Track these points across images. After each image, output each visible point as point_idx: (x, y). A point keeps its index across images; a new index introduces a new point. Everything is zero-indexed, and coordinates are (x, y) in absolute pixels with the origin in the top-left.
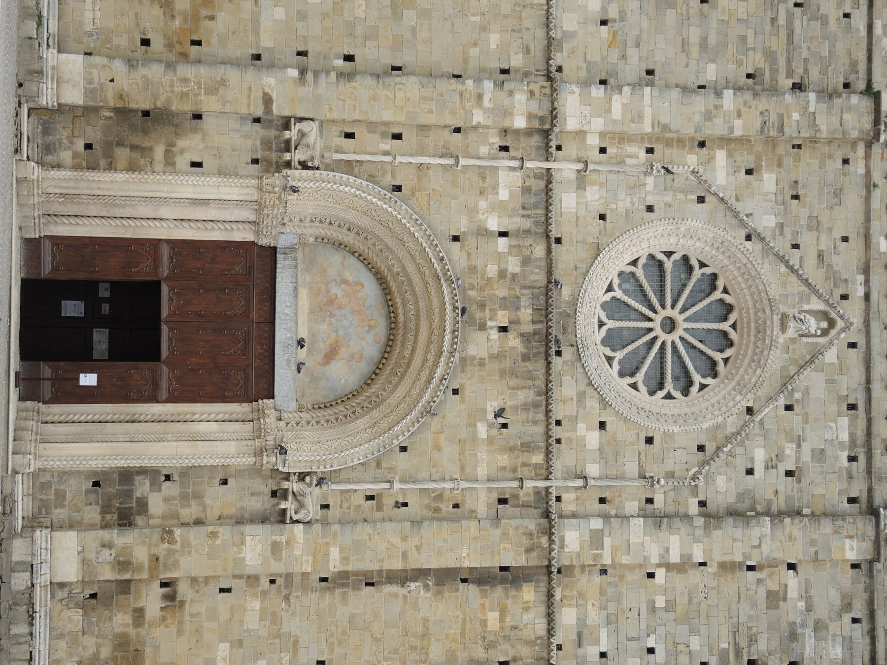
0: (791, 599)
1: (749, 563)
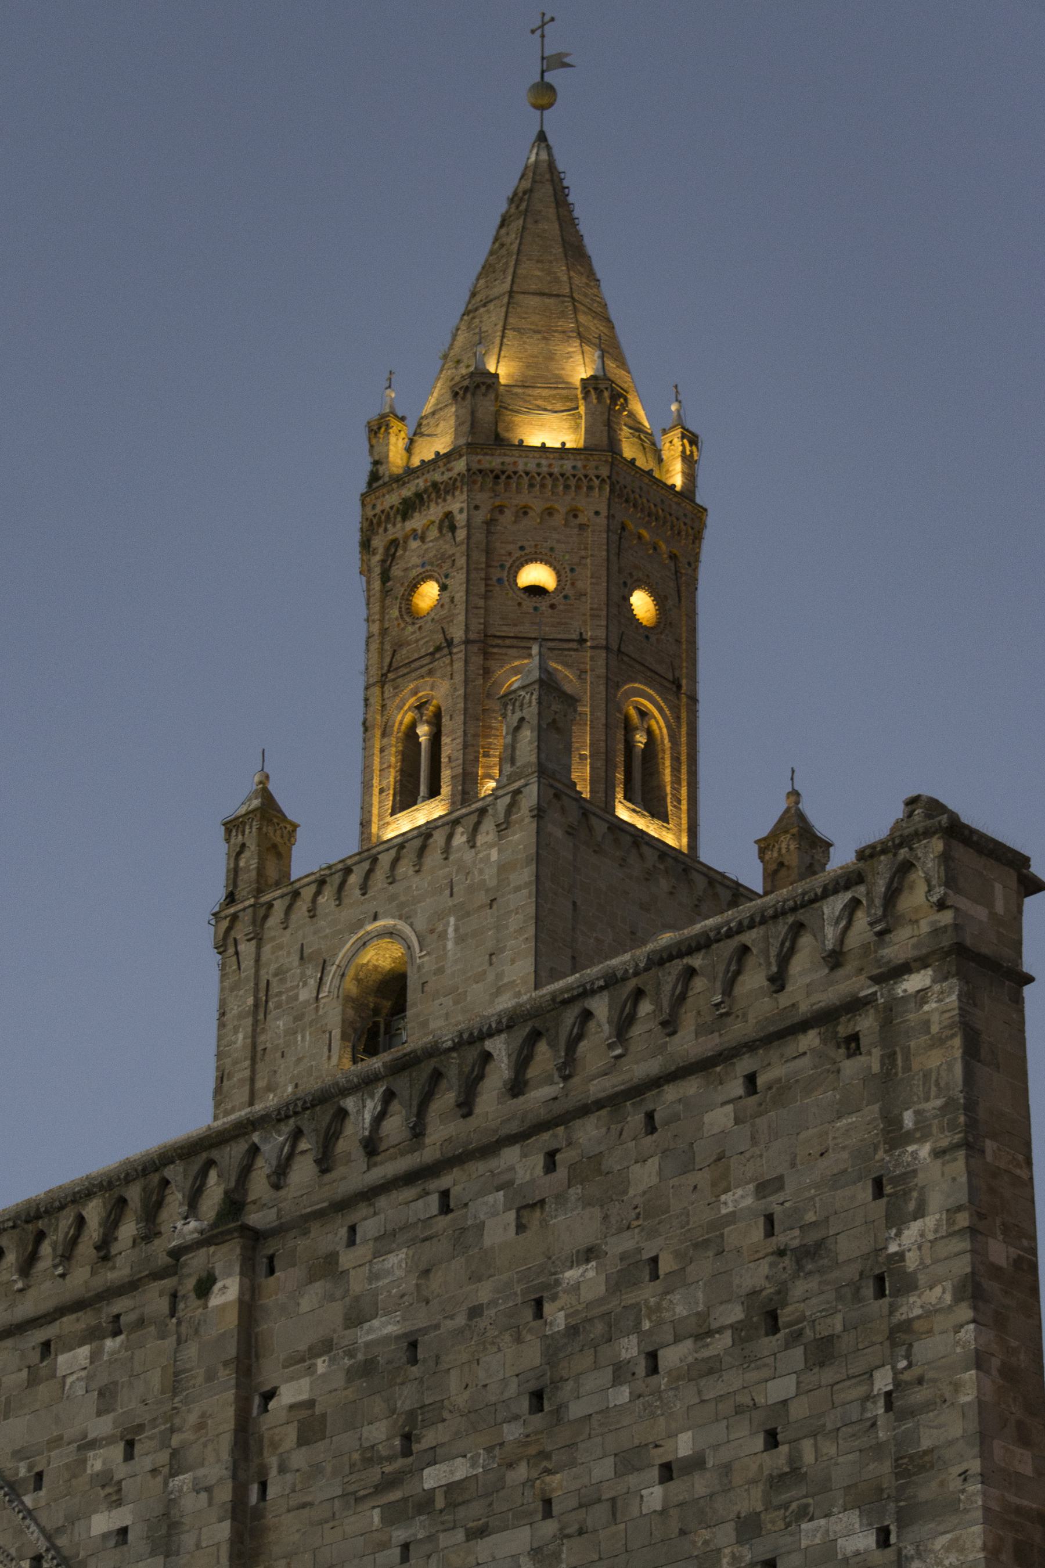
0: (311, 1390)
1: (254, 1497)
